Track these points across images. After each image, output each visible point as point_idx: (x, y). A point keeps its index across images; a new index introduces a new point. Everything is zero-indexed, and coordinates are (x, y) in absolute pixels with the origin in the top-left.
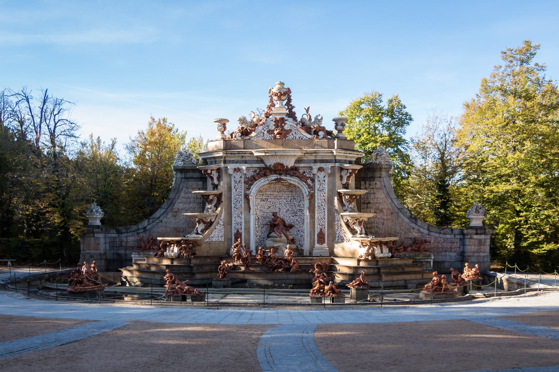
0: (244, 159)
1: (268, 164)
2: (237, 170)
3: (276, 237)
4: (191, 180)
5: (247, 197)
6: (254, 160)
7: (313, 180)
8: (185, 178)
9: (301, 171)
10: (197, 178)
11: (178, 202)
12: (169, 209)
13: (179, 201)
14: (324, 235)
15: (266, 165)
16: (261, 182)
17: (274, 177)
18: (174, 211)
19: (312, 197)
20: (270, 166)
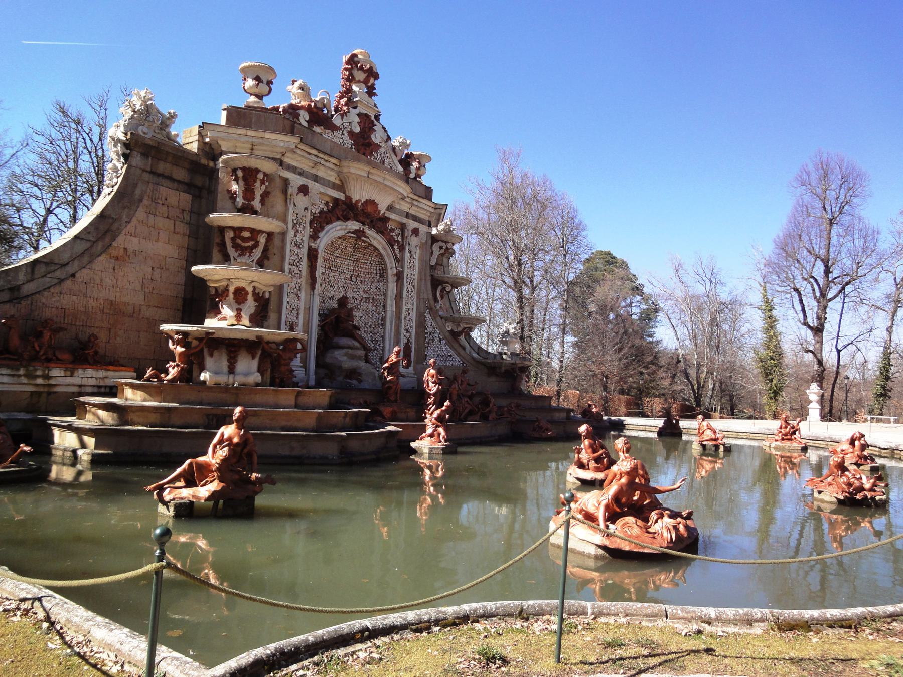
0: (314, 171)
1: (355, 197)
2: (304, 190)
3: (357, 348)
4: (163, 181)
5: (312, 255)
6: (329, 181)
7: (402, 248)
8: (152, 172)
9: (390, 225)
10: (179, 182)
11: (123, 232)
12: (100, 245)
13: (130, 228)
14: (411, 348)
15: (349, 198)
16: (336, 230)
17: (354, 225)
18: (114, 253)
19: (399, 276)
20: (360, 200)
